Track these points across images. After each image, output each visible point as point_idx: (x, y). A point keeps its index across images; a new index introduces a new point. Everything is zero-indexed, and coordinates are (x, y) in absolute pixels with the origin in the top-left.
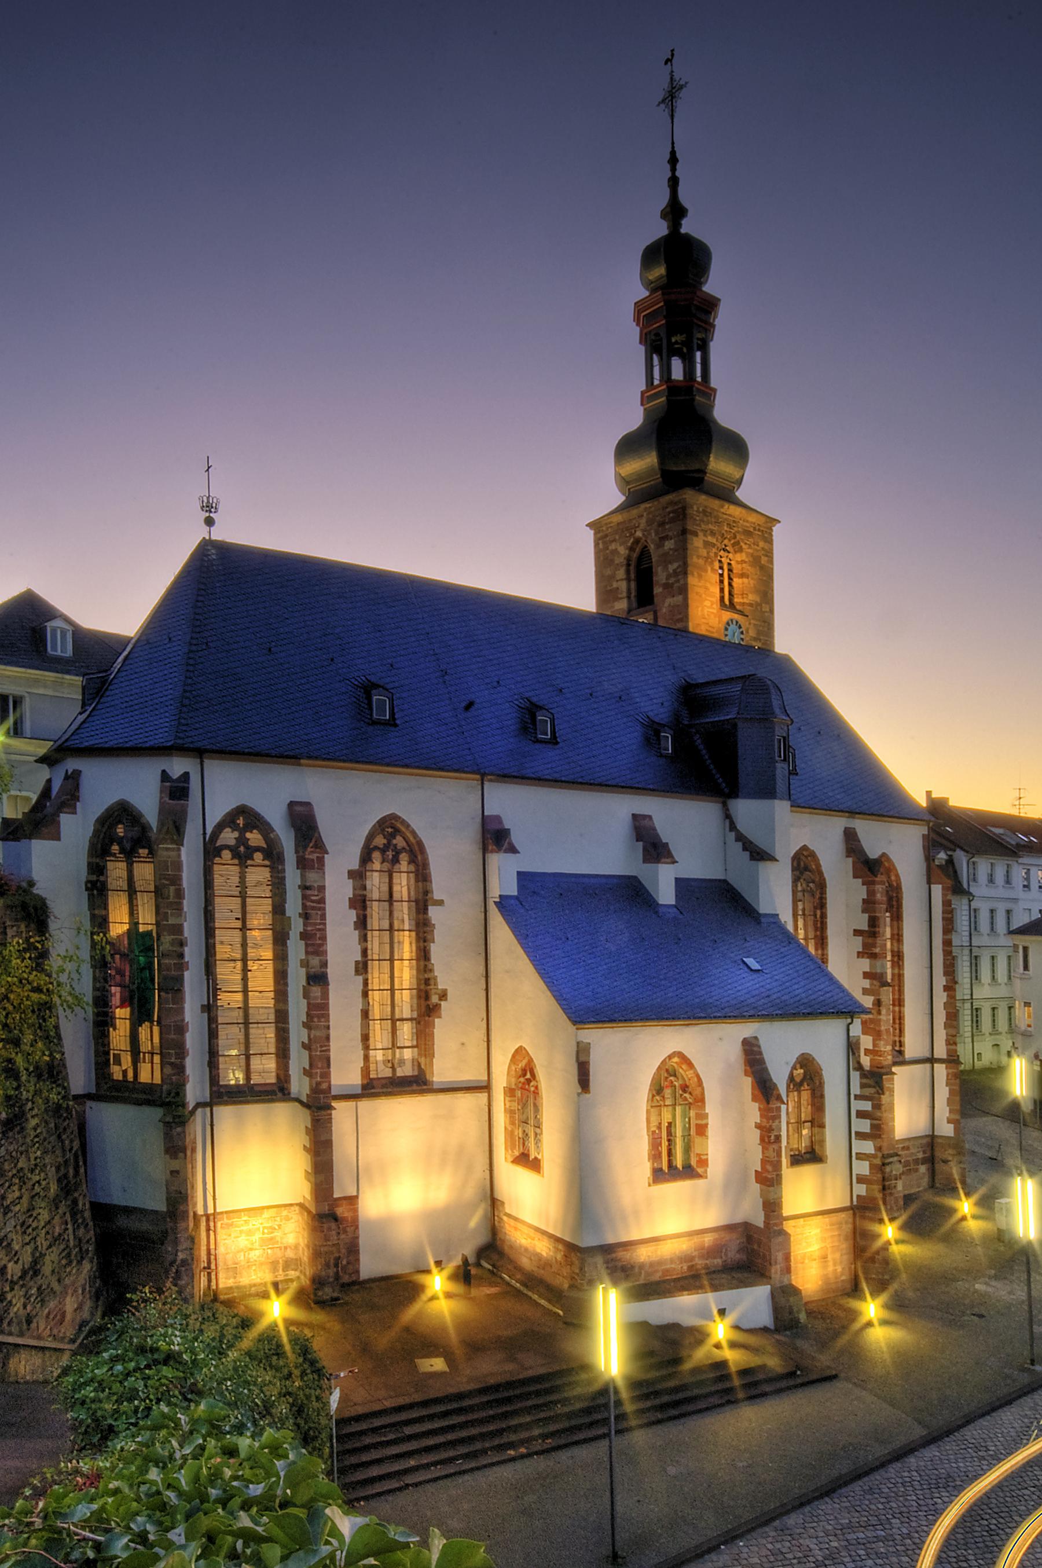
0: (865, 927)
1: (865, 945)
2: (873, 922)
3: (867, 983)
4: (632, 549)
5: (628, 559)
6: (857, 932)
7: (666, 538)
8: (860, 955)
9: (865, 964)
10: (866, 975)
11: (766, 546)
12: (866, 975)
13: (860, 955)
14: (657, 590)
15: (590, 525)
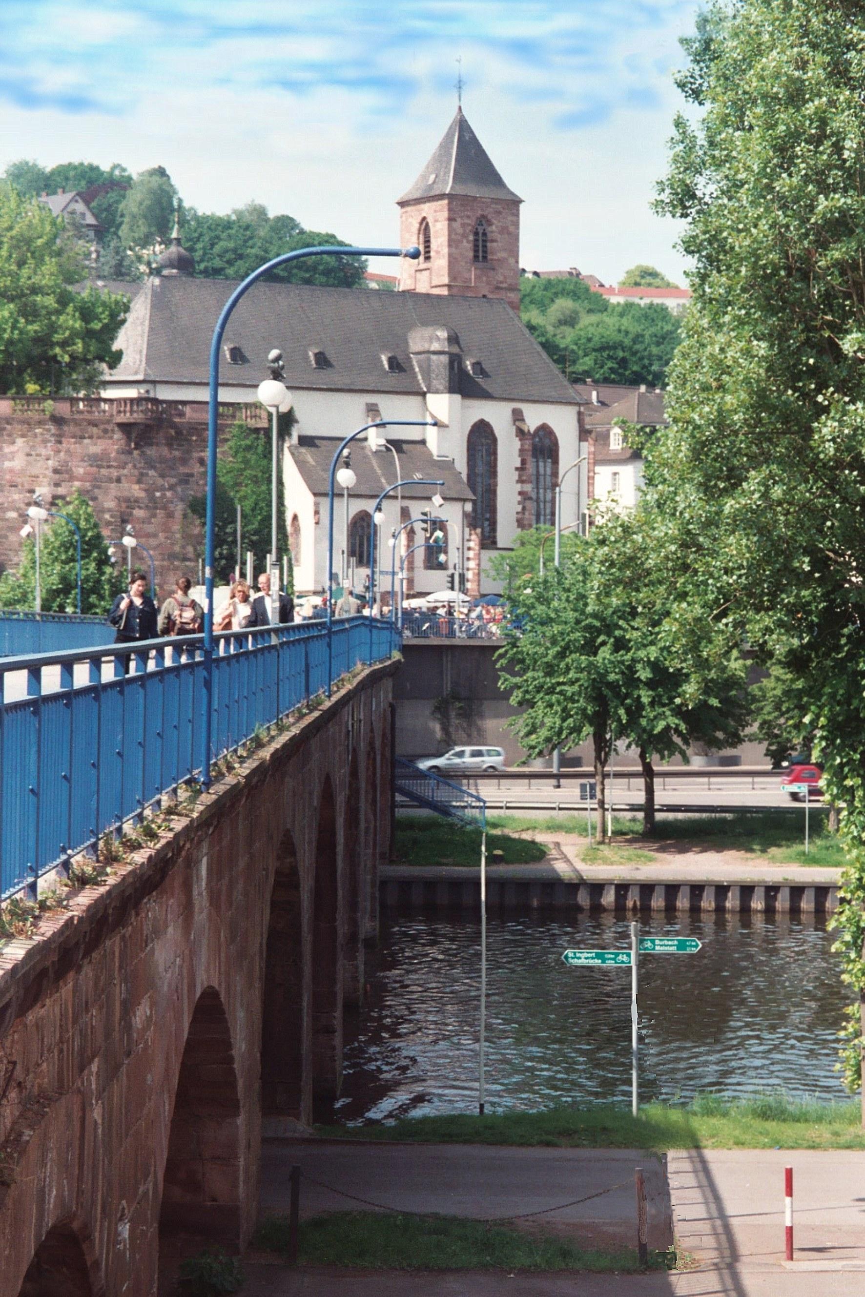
0: (519, 465)
1: (520, 476)
2: (523, 462)
3: (519, 498)
4: (421, 224)
5: (419, 230)
6: (517, 469)
7: (436, 221)
8: (518, 482)
9: (518, 487)
10: (520, 493)
11: (514, 219)
12: (520, 493)
13: (518, 482)
14: (432, 254)
15: (399, 203)
